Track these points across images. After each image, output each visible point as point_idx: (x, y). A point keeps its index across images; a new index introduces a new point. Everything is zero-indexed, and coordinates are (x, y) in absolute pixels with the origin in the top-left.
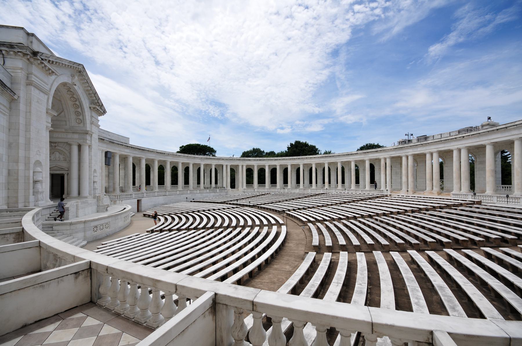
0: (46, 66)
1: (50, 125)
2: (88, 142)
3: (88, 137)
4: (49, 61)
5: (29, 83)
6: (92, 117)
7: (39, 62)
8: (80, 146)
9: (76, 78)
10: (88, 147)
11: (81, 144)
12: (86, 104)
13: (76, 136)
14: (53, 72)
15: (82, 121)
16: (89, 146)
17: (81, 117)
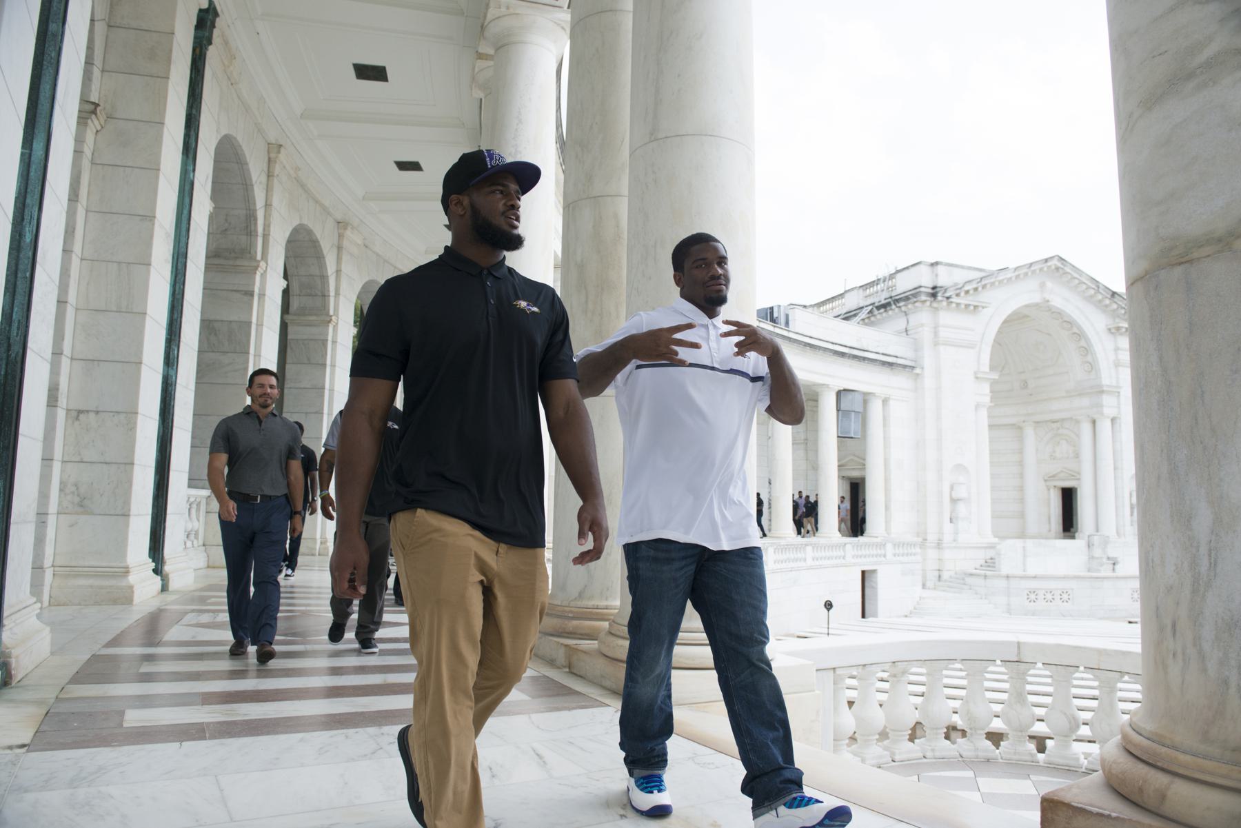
0: (958, 304)
1: (987, 399)
2: (1109, 411)
3: (1107, 400)
4: (967, 292)
5: (936, 344)
6: (1117, 349)
7: (945, 303)
8: (1094, 422)
9: (1049, 284)
10: (1109, 423)
11: (1095, 417)
12: (1095, 323)
13: (1085, 401)
14: (975, 307)
15: (1092, 367)
16: (1113, 420)
17: (1089, 358)
